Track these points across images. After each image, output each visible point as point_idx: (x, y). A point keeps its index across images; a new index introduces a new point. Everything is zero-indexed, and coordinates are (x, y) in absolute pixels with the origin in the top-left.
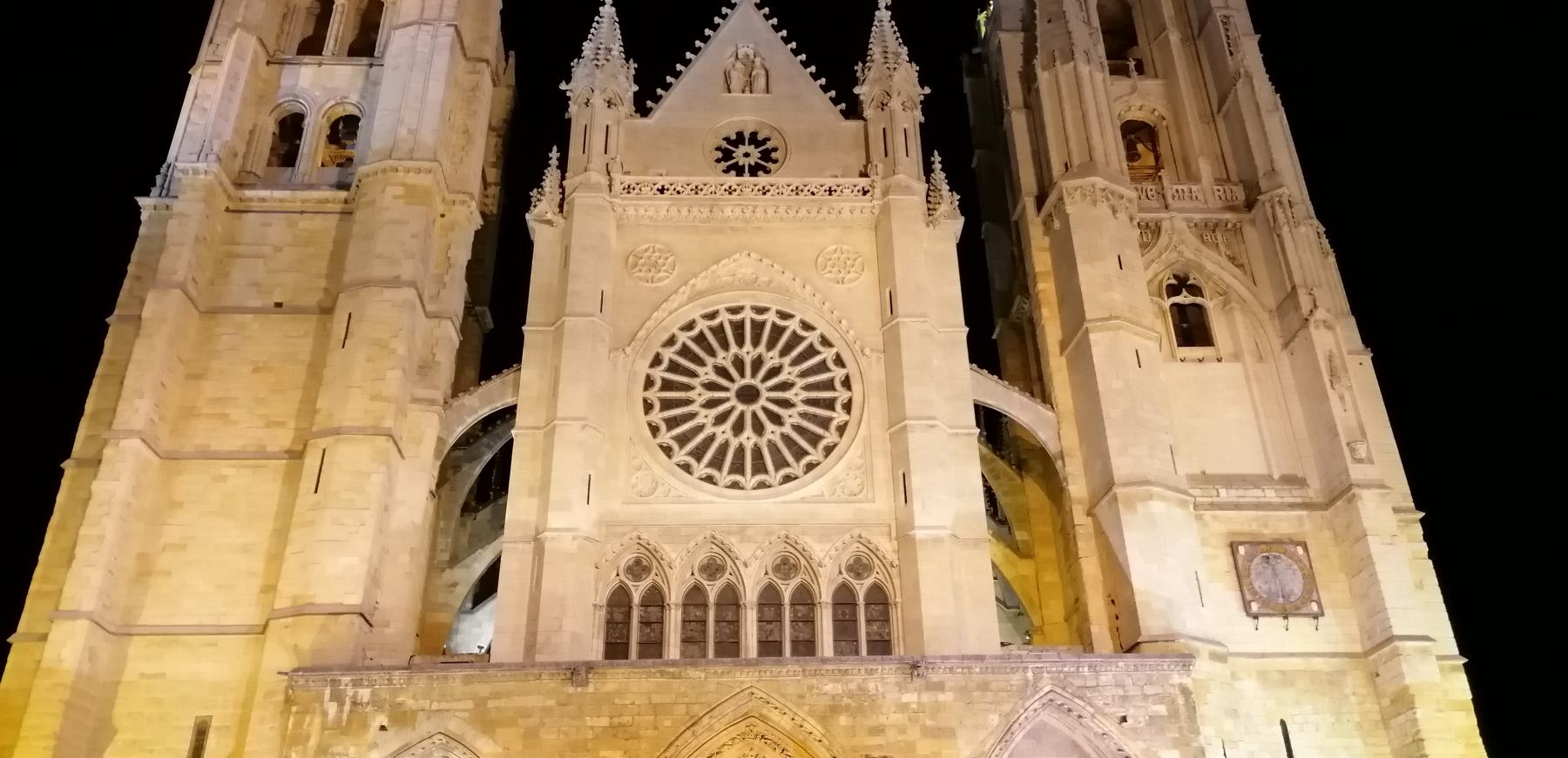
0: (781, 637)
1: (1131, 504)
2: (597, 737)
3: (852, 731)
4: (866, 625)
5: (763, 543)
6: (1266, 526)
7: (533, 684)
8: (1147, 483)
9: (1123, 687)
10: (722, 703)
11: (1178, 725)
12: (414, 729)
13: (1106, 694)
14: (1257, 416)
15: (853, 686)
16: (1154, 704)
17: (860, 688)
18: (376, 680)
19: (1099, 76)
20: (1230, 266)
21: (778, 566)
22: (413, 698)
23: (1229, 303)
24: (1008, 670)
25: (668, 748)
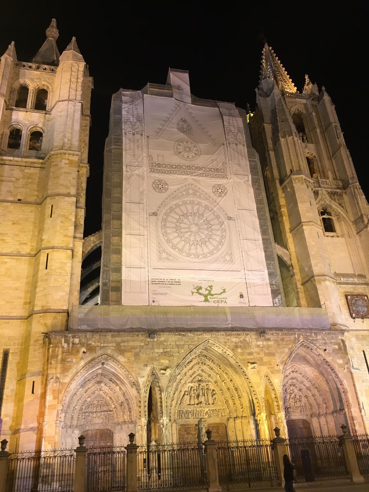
1: (319, 282)
2: (159, 356)
3: (242, 354)
6: (355, 290)
7: (136, 338)
8: (325, 275)
11: (341, 352)
12: (96, 353)
14: (350, 255)
15: (242, 339)
17: (244, 340)
19: (299, 141)
20: (339, 206)
22: (94, 342)
23: (340, 219)
24: (290, 334)
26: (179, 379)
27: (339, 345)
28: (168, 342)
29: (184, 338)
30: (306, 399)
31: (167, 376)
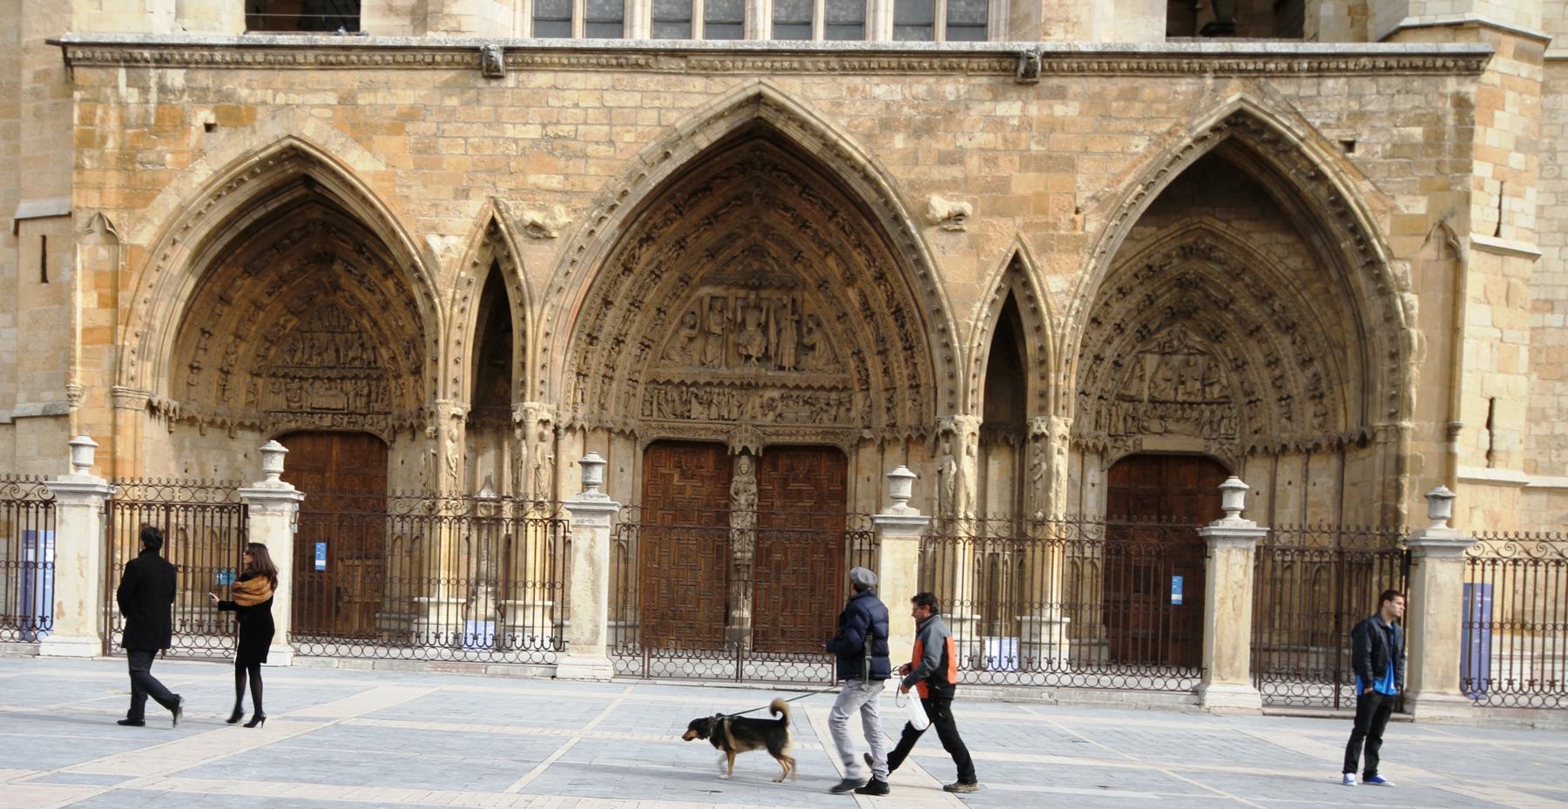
2: (523, 154)
3: (912, 159)
9: (1360, 97)
12: (254, 132)
16: (1406, 124)
17: (930, 92)
22: (248, 86)
27: (1434, 124)
28: (568, 94)
29: (641, 80)
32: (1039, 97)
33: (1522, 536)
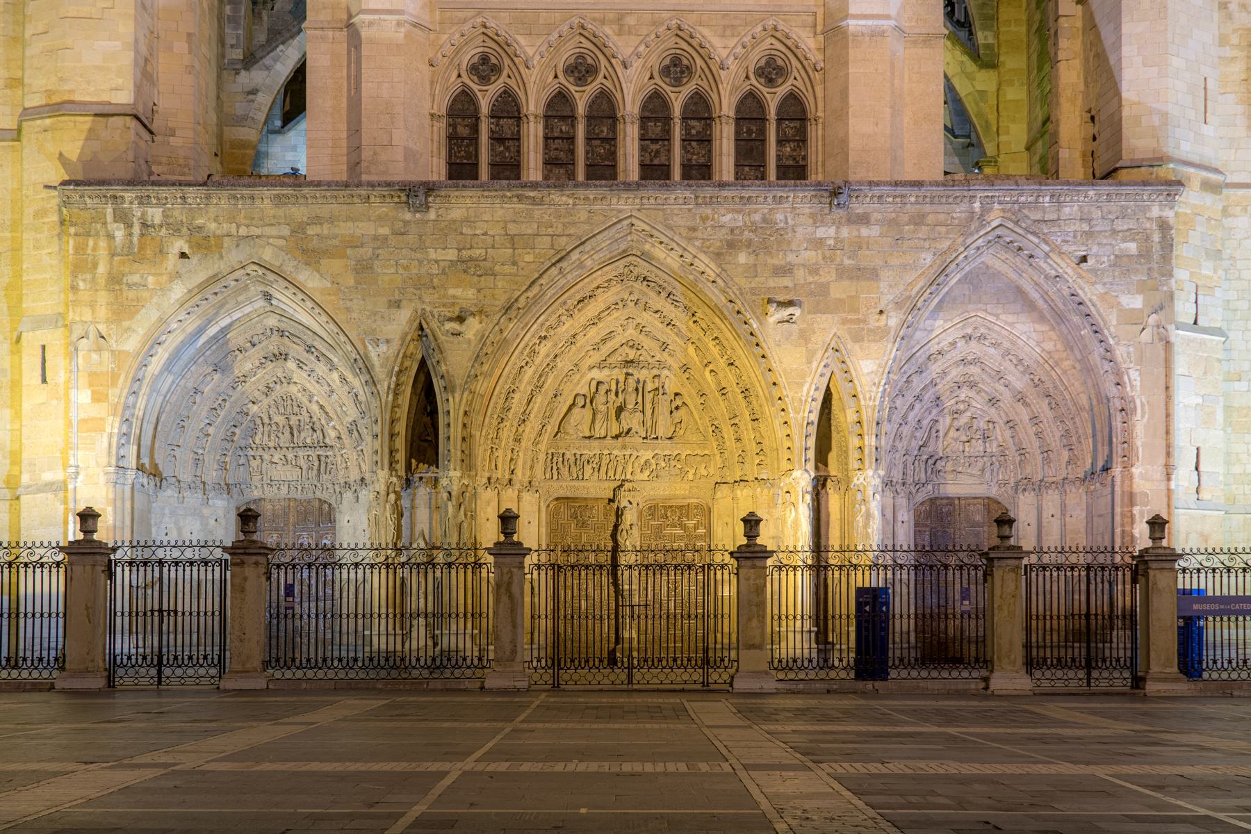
0: (669, 159)
3: (752, 271)
4: (777, 145)
5: (648, 35)
7: (360, 207)
10: (594, 236)
12: (221, 257)
13: (1067, 228)
15: (757, 217)
16: (1124, 240)
17: (764, 220)
18: (166, 198)
21: (667, 67)
22: (215, 220)
24: (951, 200)
25: (530, 286)
26: (548, 356)
29: (537, 212)
30: (1008, 433)
31: (469, 342)
32: (849, 221)
33: (1218, 551)
